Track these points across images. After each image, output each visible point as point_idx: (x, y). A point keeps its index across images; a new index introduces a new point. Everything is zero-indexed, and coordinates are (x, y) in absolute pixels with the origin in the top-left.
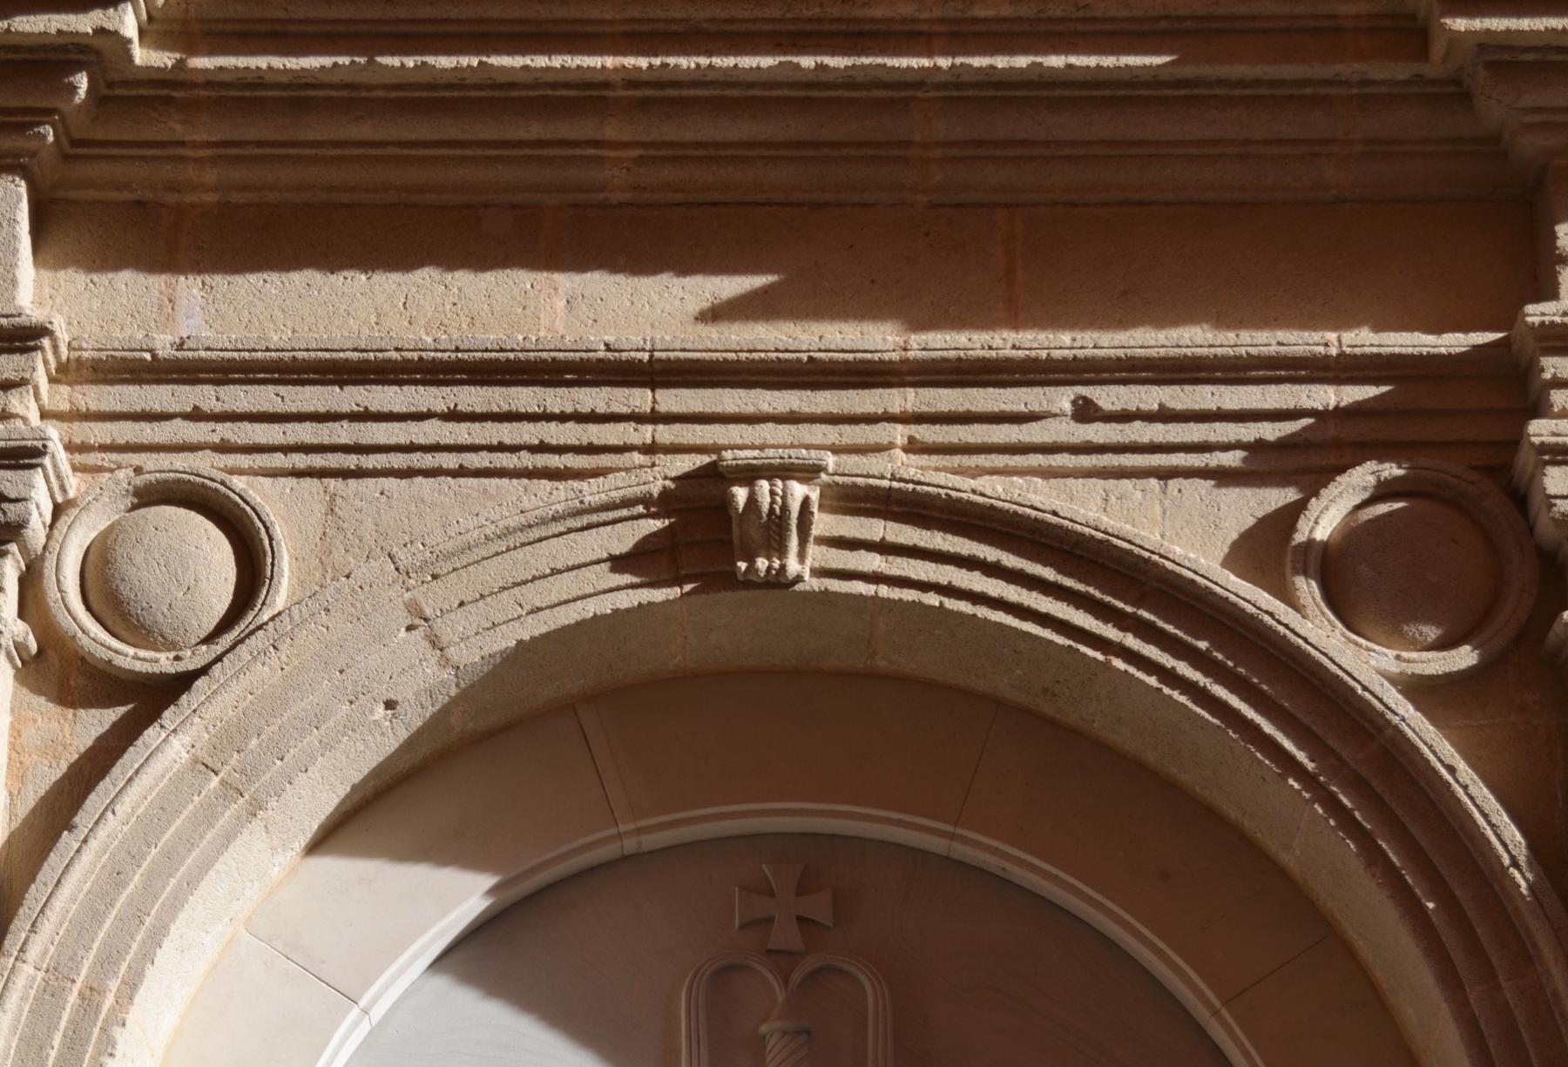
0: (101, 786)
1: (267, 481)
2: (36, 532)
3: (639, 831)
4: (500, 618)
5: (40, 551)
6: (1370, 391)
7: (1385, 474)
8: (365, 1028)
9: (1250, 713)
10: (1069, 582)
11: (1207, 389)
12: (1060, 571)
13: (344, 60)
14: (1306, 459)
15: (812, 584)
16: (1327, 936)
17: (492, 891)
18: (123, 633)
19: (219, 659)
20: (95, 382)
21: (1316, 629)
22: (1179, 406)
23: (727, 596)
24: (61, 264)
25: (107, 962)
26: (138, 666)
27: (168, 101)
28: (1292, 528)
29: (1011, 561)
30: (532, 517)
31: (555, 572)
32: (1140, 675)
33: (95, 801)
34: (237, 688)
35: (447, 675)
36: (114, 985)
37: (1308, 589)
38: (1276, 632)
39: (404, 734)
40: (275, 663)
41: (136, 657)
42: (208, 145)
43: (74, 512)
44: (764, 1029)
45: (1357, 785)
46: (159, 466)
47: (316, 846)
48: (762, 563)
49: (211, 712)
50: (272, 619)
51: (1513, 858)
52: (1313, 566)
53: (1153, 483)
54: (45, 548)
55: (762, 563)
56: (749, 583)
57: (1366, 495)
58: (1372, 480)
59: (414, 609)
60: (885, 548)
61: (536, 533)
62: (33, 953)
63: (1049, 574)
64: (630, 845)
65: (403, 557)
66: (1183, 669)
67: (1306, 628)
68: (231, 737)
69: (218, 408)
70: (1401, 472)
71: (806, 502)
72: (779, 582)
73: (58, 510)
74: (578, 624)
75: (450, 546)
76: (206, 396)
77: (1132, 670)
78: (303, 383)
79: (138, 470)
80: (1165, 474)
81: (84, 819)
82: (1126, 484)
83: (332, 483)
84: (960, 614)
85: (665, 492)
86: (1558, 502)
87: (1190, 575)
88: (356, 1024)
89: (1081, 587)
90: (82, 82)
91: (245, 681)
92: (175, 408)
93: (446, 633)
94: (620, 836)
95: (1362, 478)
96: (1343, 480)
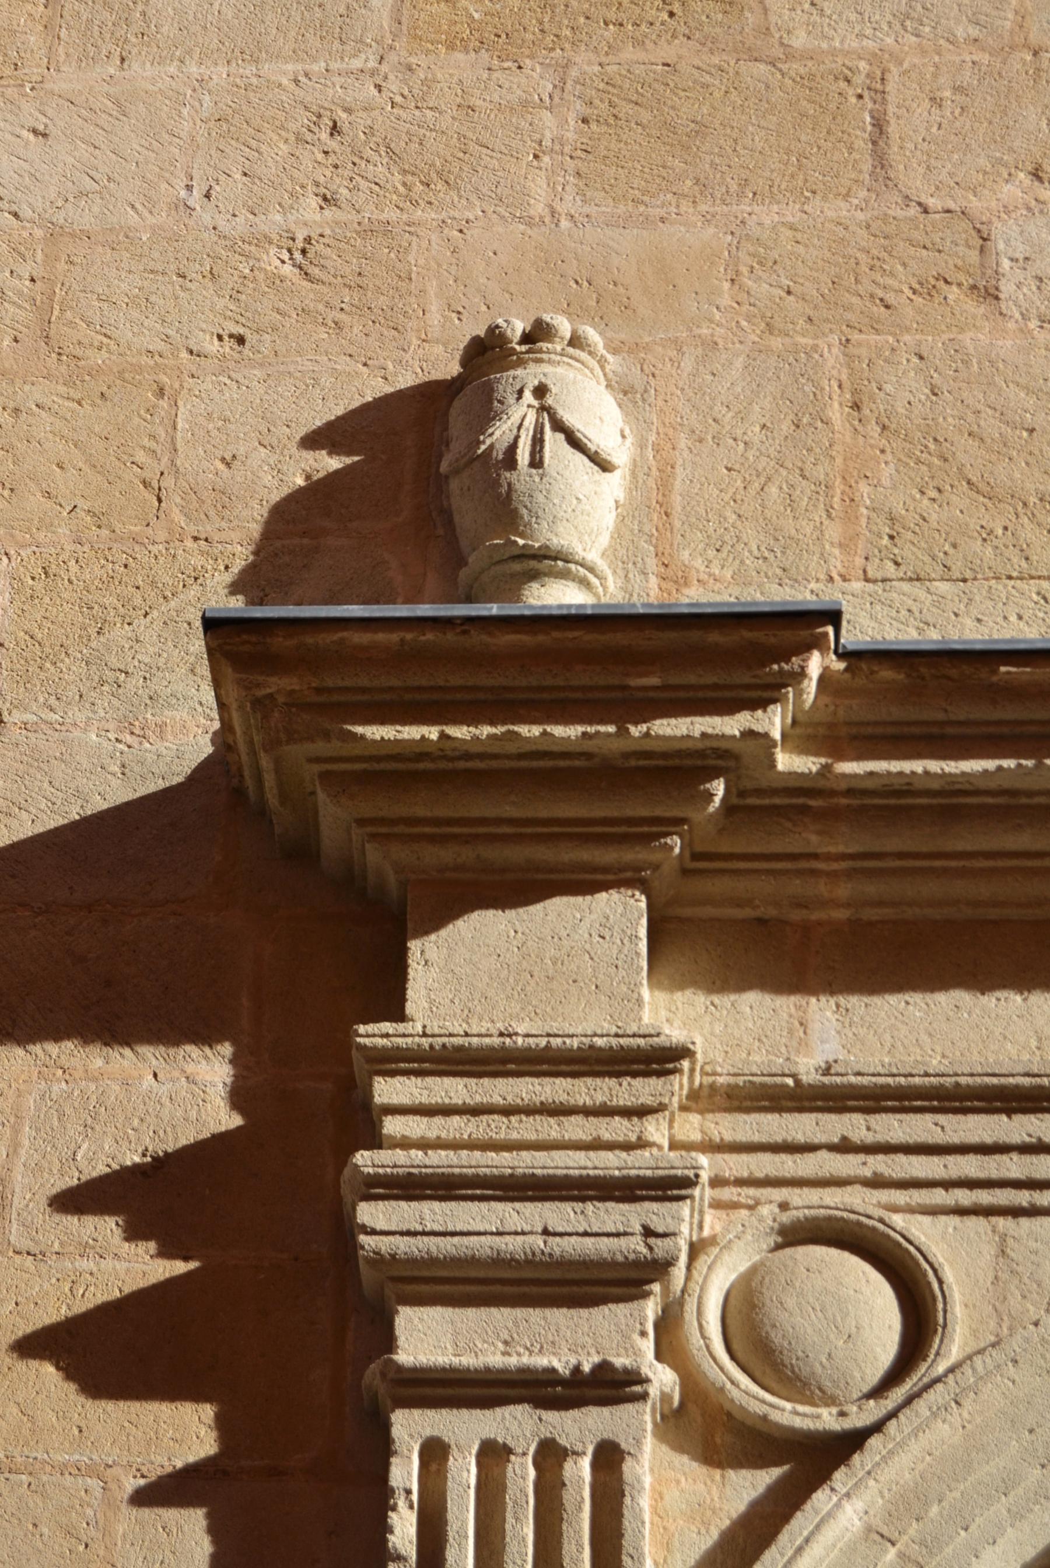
1: (926, 1220)
5: (679, 1293)
13: (1009, 763)
18: (773, 1385)
19: (893, 1415)
20: (727, 1110)
24: (679, 984)
26: (798, 1423)
27: (804, 810)
34: (915, 1448)
40: (956, 1420)
41: (795, 1413)
42: (844, 857)
43: (715, 1250)
46: (808, 1202)
49: (887, 1474)
54: (683, 1291)
68: (908, 1504)
69: (870, 1138)
76: (855, 1126)
78: (965, 1111)
79: (784, 1206)
90: (718, 788)
91: (924, 1439)
92: (820, 1138)
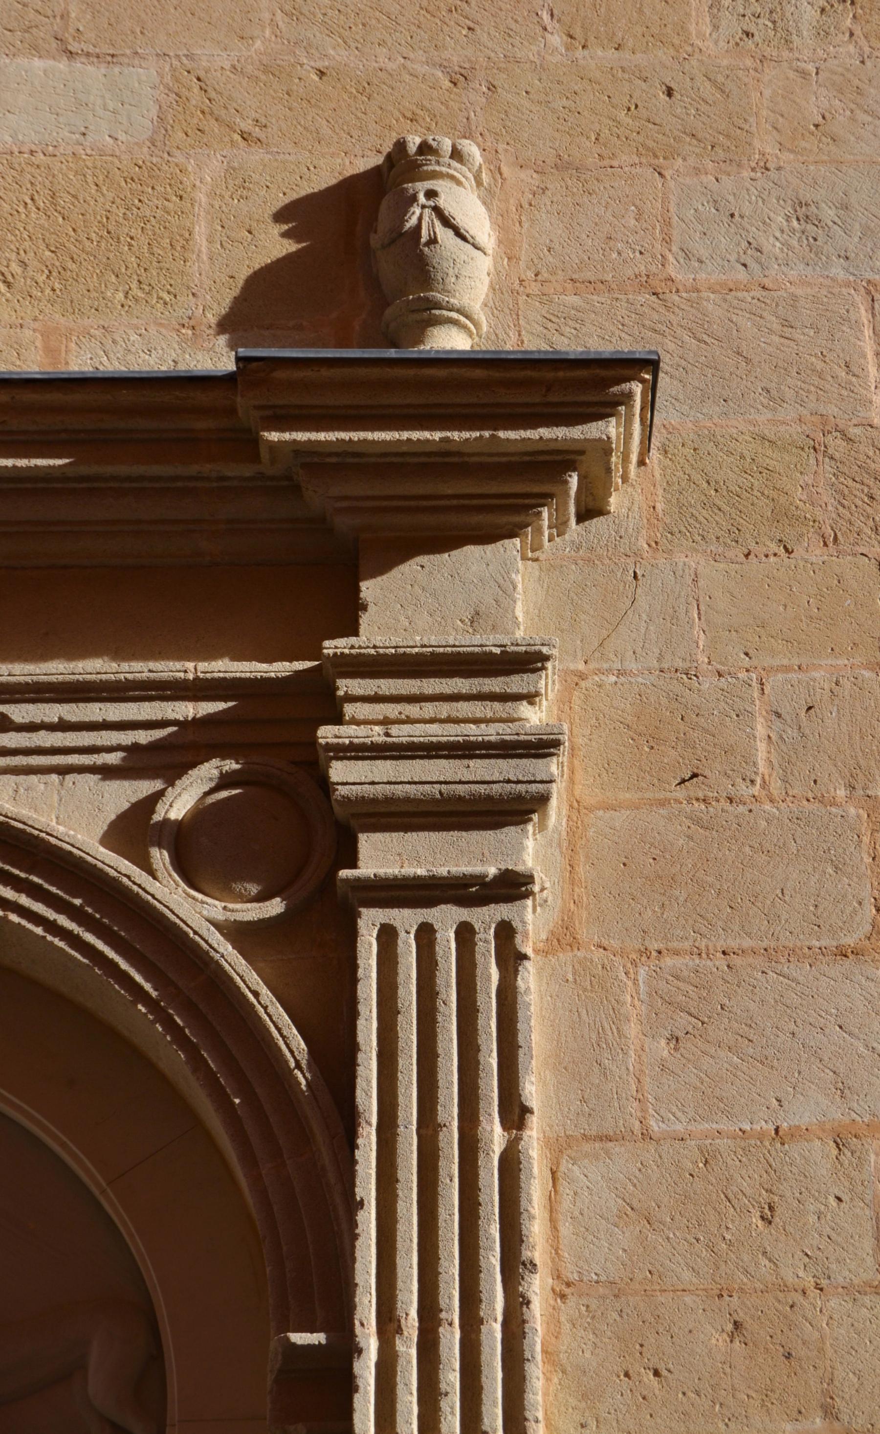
6: (221, 706)
7: (226, 768)
11: (96, 706)
14: (166, 759)
22: (73, 718)
37: (160, 857)
38: (131, 891)
51: (297, 1062)
58: (216, 773)
67: (153, 886)
70: (238, 766)
80: (63, 771)
87: (69, 848)
95: (208, 772)
96: (194, 773)
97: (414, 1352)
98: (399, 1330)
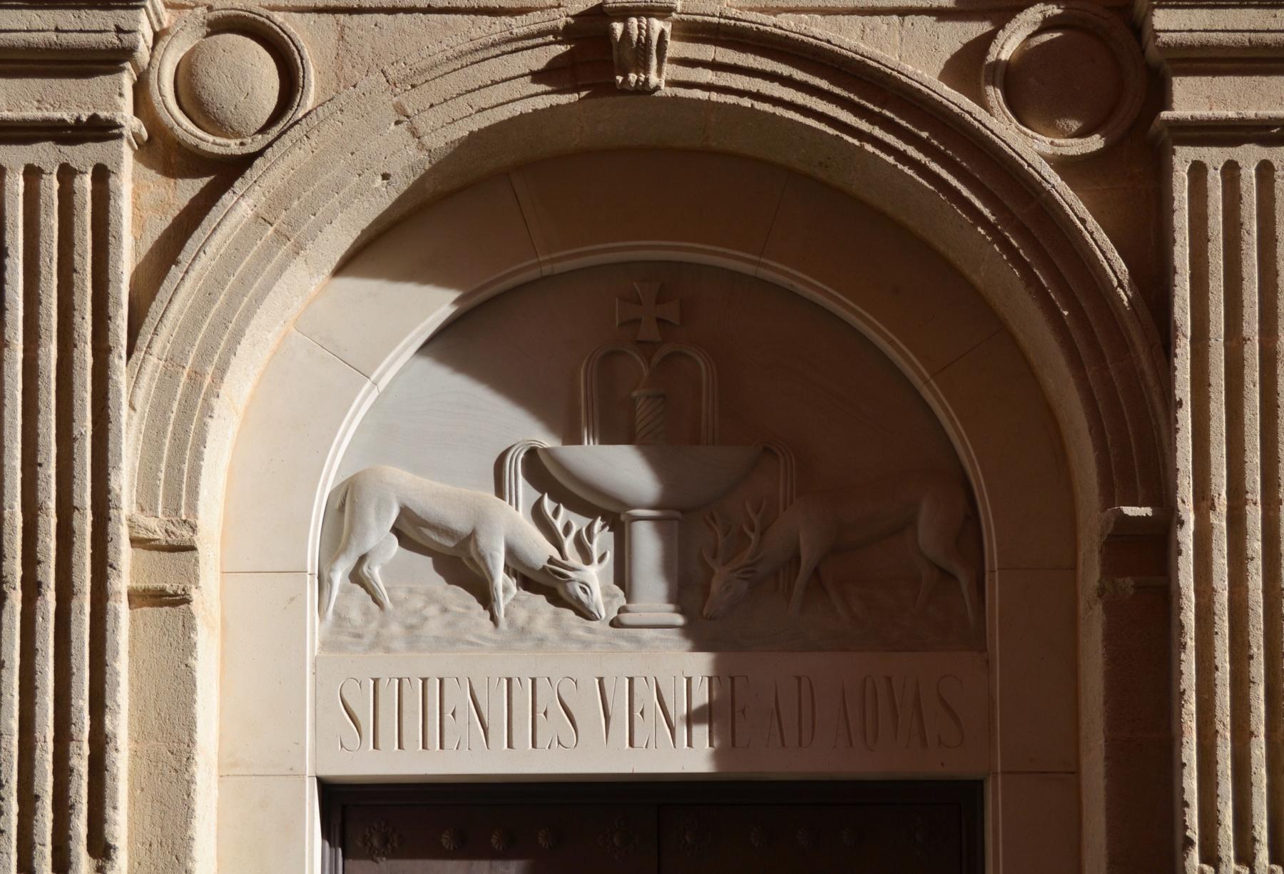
0: (196, 234)
2: (143, 54)
3: (552, 261)
4: (457, 115)
5: (146, 66)
7: (1049, 13)
8: (375, 394)
9: (954, 182)
10: (837, 90)
12: (831, 83)
15: (666, 91)
16: (1000, 331)
17: (456, 302)
18: (206, 126)
19: (270, 145)
21: (1000, 125)
23: (609, 100)
25: (205, 355)
26: (216, 150)
28: (986, 51)
29: (799, 75)
30: (477, 44)
31: (494, 83)
32: (883, 155)
33: (192, 245)
34: (283, 166)
35: (423, 156)
36: (210, 370)
37: (994, 95)
38: (973, 126)
39: (395, 196)
40: (307, 147)
41: (214, 143)
43: (168, 38)
44: (635, 394)
45: (1022, 232)
47: (339, 271)
48: (633, 77)
49: (266, 182)
50: (305, 116)
51: (1119, 281)
52: (999, 78)
53: (895, 18)
54: (149, 64)
55: (633, 77)
56: (625, 90)
57: (1036, 28)
58: (1040, 17)
59: (400, 109)
60: (715, 66)
61: (481, 55)
62: (156, 348)
63: (824, 84)
64: (547, 269)
65: (391, 72)
66: (912, 151)
67: (992, 123)
68: (280, 200)
70: (1058, 11)
71: (662, 33)
72: (644, 90)
73: (157, 37)
74: (510, 120)
75: (423, 64)
77: (878, 152)
81: (185, 257)
82: (877, 19)
83: (342, 18)
84: (765, 113)
85: (567, 25)
86: (1161, 34)
87: (918, 85)
88: (369, 392)
89: (845, 94)
91: (289, 160)
93: (422, 128)
94: (540, 264)
97: (1224, 524)
98: (1213, 507)
